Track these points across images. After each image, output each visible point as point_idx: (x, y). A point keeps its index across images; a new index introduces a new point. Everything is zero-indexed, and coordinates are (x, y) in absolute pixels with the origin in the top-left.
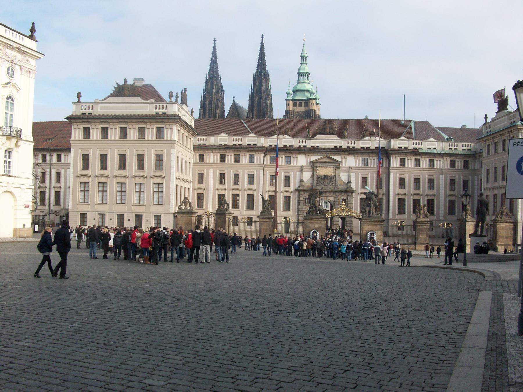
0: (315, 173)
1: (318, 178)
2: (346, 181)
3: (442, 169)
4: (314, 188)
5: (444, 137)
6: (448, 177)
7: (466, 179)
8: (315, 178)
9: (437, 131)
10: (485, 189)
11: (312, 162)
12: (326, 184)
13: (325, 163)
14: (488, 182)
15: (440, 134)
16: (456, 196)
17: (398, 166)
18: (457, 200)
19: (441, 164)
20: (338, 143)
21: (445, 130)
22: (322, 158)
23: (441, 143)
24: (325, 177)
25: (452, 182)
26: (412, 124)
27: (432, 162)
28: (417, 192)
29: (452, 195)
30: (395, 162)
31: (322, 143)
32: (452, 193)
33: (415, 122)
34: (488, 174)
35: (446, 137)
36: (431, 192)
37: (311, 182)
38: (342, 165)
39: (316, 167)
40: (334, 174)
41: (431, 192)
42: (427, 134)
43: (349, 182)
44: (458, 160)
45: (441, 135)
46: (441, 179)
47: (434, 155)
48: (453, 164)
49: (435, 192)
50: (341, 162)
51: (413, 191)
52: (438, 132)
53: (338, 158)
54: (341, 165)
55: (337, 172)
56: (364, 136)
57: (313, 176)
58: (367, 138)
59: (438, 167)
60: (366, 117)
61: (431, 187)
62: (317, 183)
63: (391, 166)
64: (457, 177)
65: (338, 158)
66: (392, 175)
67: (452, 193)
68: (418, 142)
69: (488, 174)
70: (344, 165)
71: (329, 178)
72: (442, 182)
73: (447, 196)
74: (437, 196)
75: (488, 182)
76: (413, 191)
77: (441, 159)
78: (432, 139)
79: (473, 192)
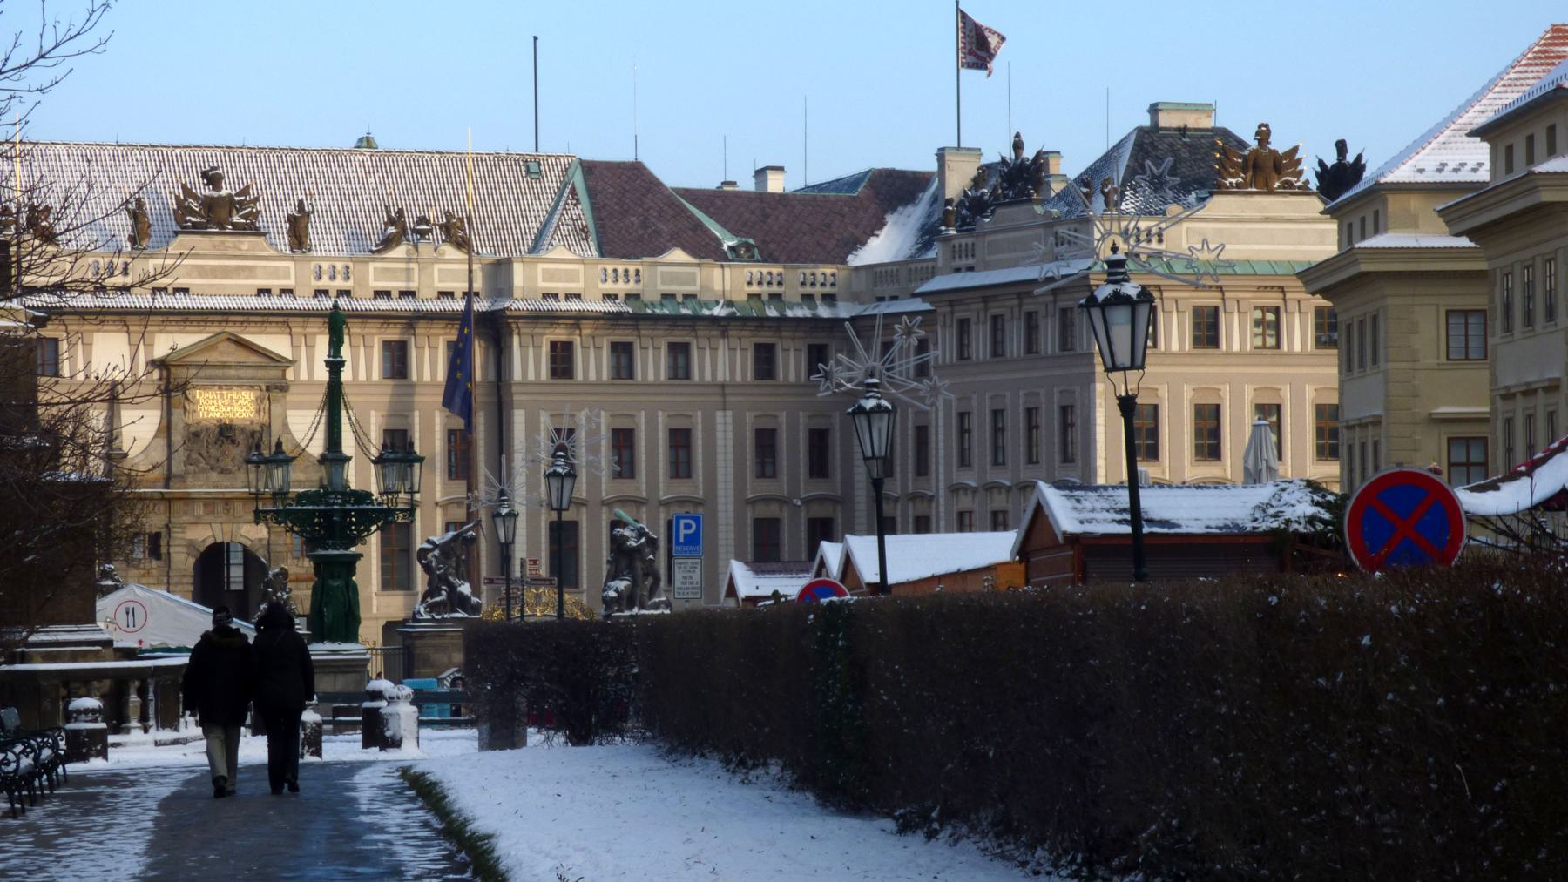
0: (177, 414)
1: (194, 435)
2: (317, 448)
3: (723, 386)
4: (175, 490)
5: (719, 243)
6: (749, 417)
7: (819, 424)
8: (177, 438)
9: (685, 210)
10: (955, 490)
11: (162, 364)
12: (227, 462)
13: (224, 366)
14: (964, 461)
15: (699, 225)
16: (782, 501)
17: (544, 374)
18: (785, 516)
19: (722, 362)
20: (275, 273)
21: (721, 202)
22: (206, 346)
23: (717, 272)
24: (225, 432)
25: (766, 441)
26: (578, 179)
27: (679, 352)
28: (626, 488)
29: (767, 500)
30: (528, 361)
31: (203, 272)
32: (766, 487)
33: (589, 168)
34: (964, 431)
35: (728, 242)
36: (683, 489)
37: (159, 455)
38: (297, 373)
39: (183, 387)
40: (264, 418)
41: (683, 489)
42: (645, 224)
43: (333, 456)
44: (789, 344)
45: (706, 231)
46: (720, 427)
47: (694, 321)
48: (765, 362)
49: (694, 488)
50: (291, 362)
51: (607, 488)
52: (692, 217)
53: (276, 343)
54: (290, 375)
55: (276, 409)
56: (388, 243)
57: (166, 429)
58: (400, 251)
59: (708, 378)
60: (367, 142)
61: (681, 466)
62: (189, 461)
63: (517, 375)
64: (783, 417)
65: (276, 343)
66: (519, 418)
67: (766, 487)
68: (621, 269)
69: (964, 431)
70: (304, 376)
71: (240, 439)
72: (723, 442)
73: (743, 503)
74: (707, 502)
75: (964, 461)
76: (607, 488)
77: (722, 345)
78: (678, 255)
79: (848, 483)
